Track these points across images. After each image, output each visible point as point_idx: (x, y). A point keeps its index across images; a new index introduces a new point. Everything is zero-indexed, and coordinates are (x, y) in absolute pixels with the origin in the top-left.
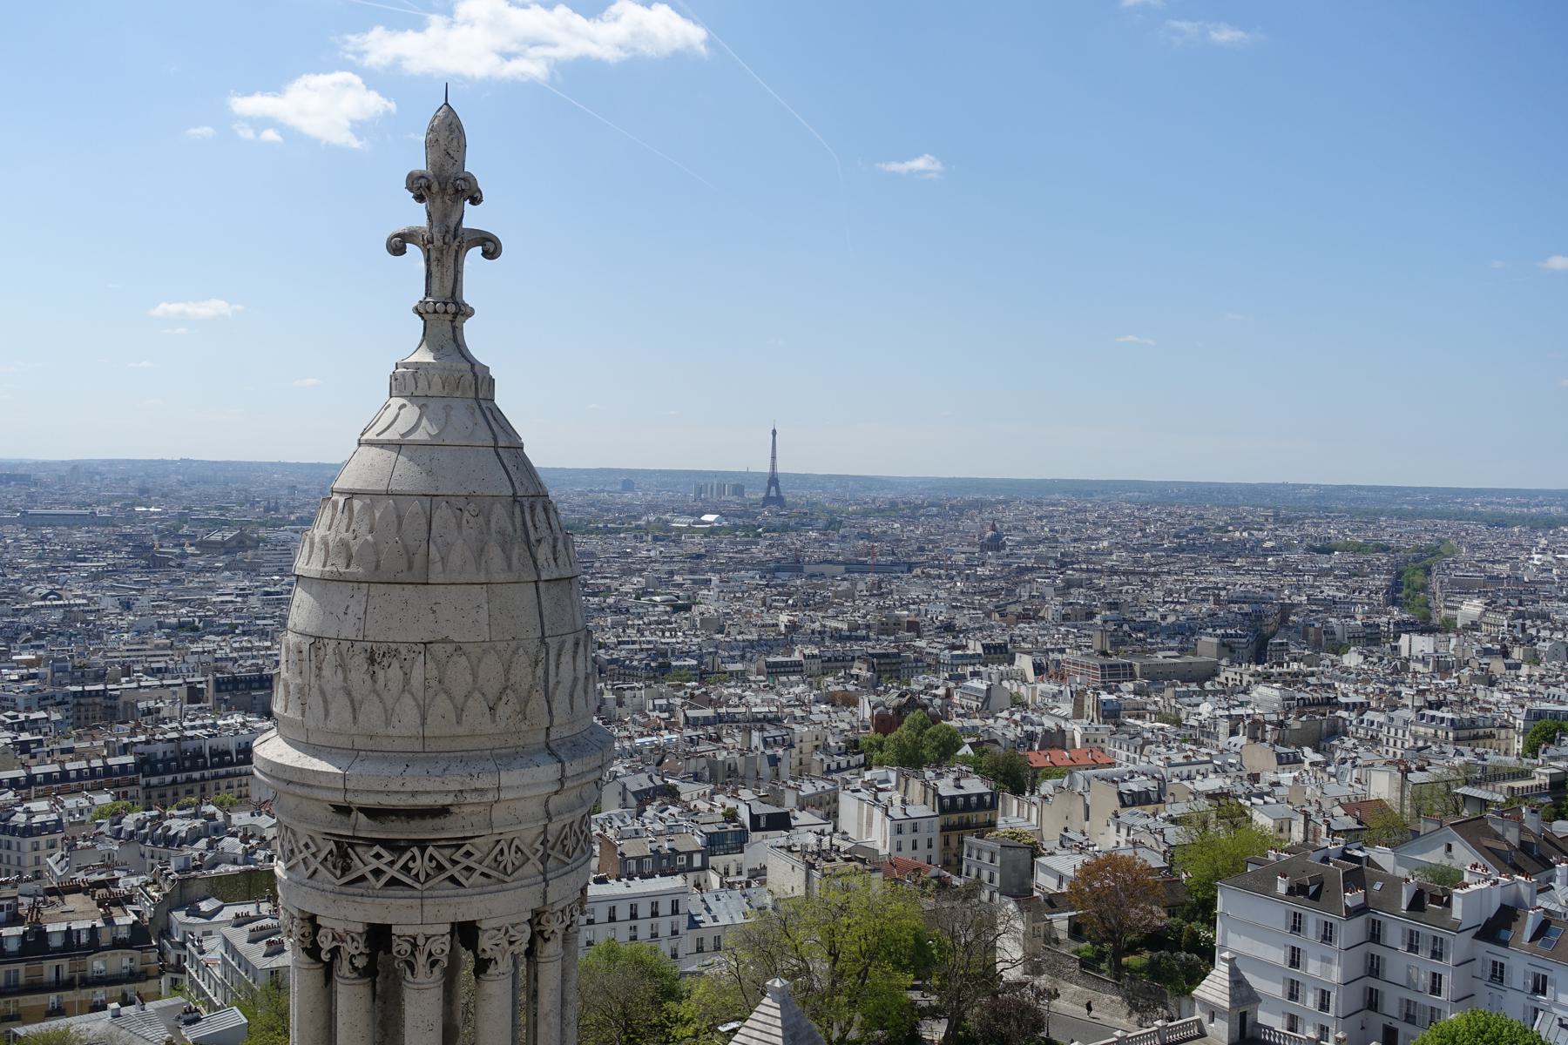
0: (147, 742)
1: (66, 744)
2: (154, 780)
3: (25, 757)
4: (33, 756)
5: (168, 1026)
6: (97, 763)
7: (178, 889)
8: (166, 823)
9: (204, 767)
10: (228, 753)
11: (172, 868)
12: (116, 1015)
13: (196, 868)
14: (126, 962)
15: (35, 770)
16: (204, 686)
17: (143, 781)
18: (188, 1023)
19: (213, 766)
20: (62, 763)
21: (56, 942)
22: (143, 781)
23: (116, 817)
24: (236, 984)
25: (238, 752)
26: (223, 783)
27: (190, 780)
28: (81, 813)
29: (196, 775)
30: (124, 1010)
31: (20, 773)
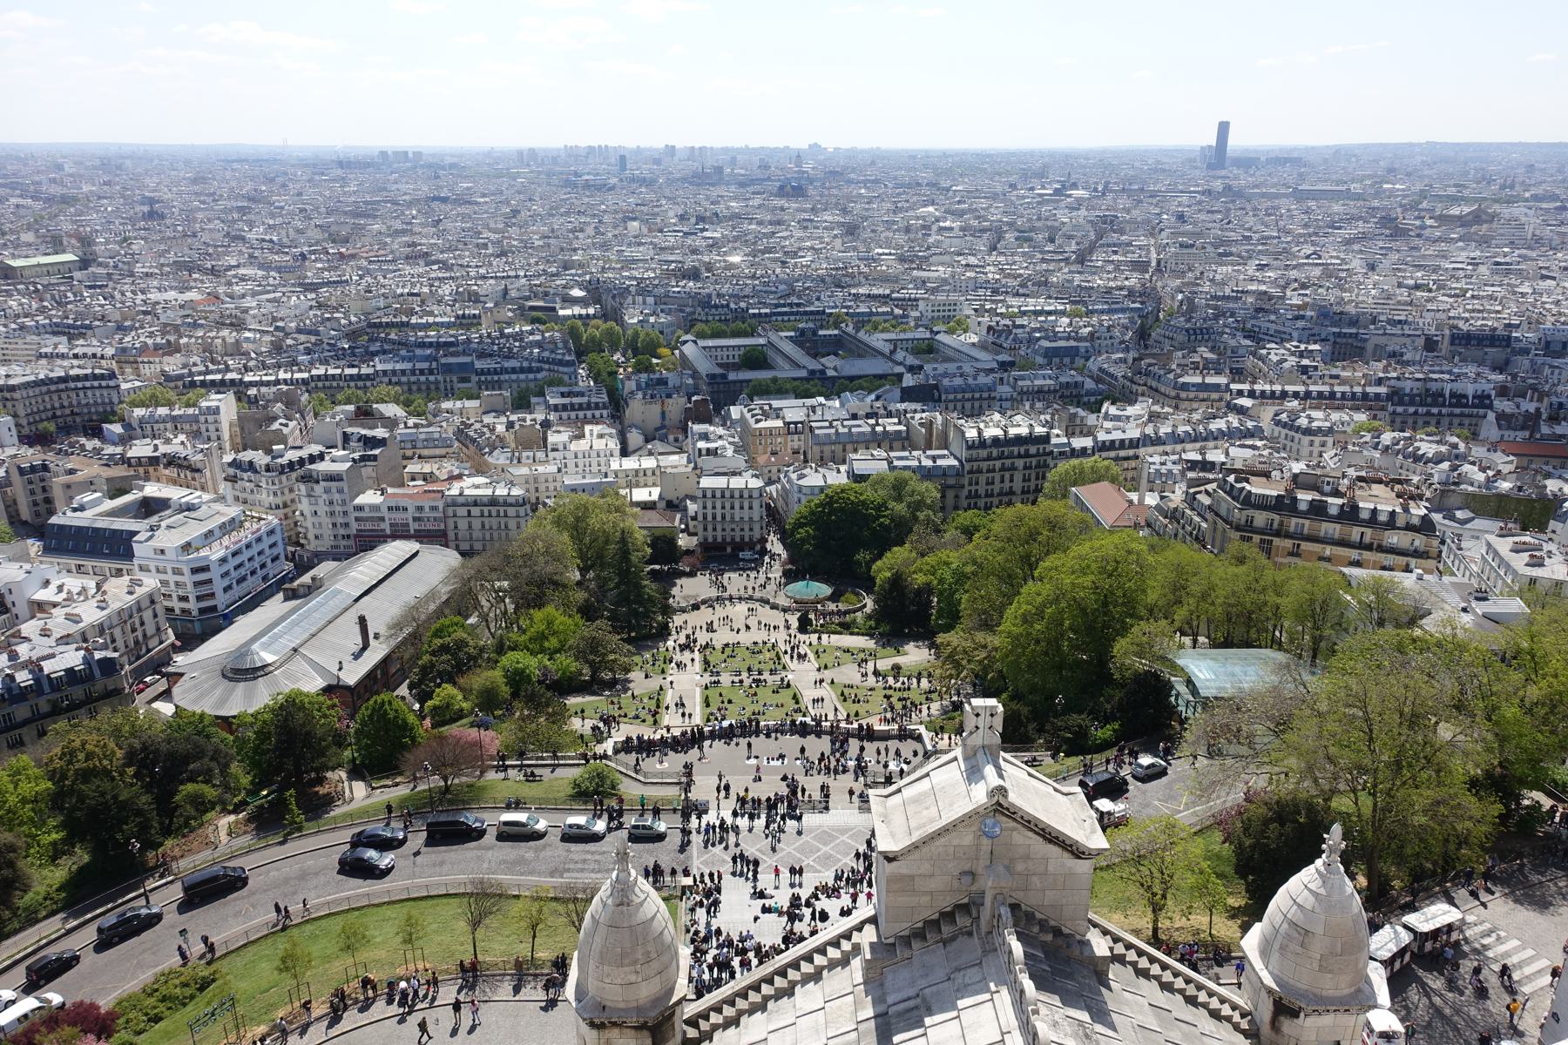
0: (1398, 379)
1: (1334, 372)
2: (1400, 409)
3: (1304, 377)
4: (1310, 378)
5: (1461, 597)
6: (1358, 389)
7: (1437, 499)
8: (1416, 444)
9: (1443, 405)
10: (1465, 396)
11: (1436, 479)
12: (1420, 578)
13: (1455, 484)
14: (1417, 543)
15: (1312, 388)
16: (1439, 338)
17: (1390, 408)
18: (1477, 599)
19: (1451, 405)
20: (1332, 385)
21: (1365, 515)
22: (1390, 408)
23: (1377, 433)
24: (1492, 579)
25: (1474, 397)
26: (1456, 421)
27: (1428, 414)
28: (1343, 424)
29: (1435, 410)
30: (1426, 577)
31: (1301, 389)
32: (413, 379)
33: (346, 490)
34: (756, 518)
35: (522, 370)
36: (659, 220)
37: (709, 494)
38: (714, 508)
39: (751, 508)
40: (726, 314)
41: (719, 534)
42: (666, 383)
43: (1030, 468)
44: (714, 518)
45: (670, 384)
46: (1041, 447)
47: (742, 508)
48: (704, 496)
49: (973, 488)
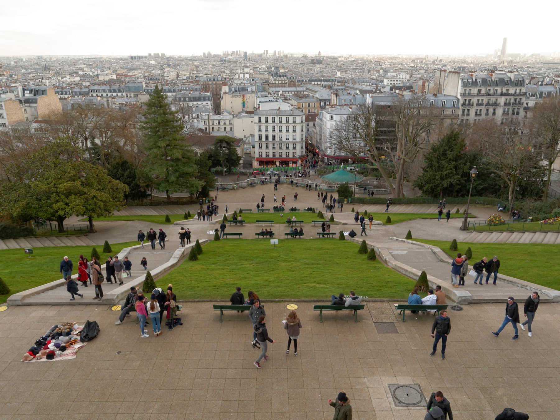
32: (109, 94)
33: (5, 116)
34: (298, 139)
36: (258, 69)
37: (263, 120)
38: (267, 131)
39: (294, 131)
40: (285, 80)
41: (271, 151)
42: (247, 90)
43: (509, 104)
44: (267, 138)
45: (249, 89)
46: (518, 89)
47: (287, 131)
48: (260, 121)
49: (465, 118)
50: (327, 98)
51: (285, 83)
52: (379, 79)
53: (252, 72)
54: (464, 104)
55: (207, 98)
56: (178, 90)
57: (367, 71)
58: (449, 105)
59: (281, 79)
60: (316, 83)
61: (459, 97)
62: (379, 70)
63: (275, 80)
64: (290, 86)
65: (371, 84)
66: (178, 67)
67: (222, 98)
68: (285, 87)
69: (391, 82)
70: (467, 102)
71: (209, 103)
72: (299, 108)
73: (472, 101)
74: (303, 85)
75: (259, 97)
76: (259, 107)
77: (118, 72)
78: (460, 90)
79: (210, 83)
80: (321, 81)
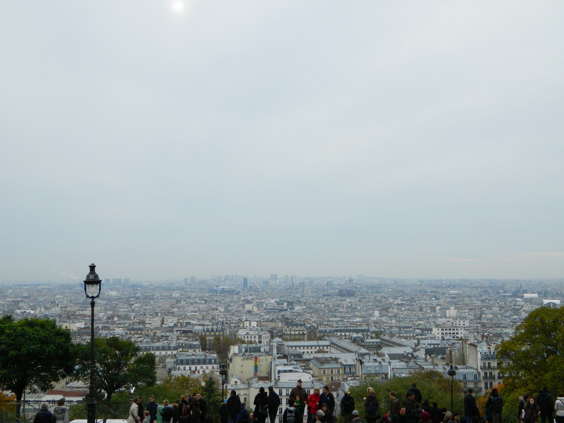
35: (163, 349)
36: (264, 305)
42: (260, 351)
45: (262, 350)
50: (353, 363)
51: (304, 334)
52: (428, 326)
53: (255, 309)
54: (485, 377)
55: (213, 361)
56: (174, 347)
57: (418, 309)
58: (470, 378)
59: (297, 329)
60: (343, 334)
61: (480, 370)
62: (435, 307)
63: (290, 330)
64: (310, 339)
65: (415, 335)
66: (152, 302)
67: (231, 360)
68: (303, 340)
69: (443, 332)
70: (488, 375)
71: (215, 366)
72: (319, 380)
73: (493, 374)
74: (326, 338)
75: (277, 365)
76: (279, 379)
77: (68, 309)
78: (480, 364)
79: (208, 334)
80: (350, 331)
